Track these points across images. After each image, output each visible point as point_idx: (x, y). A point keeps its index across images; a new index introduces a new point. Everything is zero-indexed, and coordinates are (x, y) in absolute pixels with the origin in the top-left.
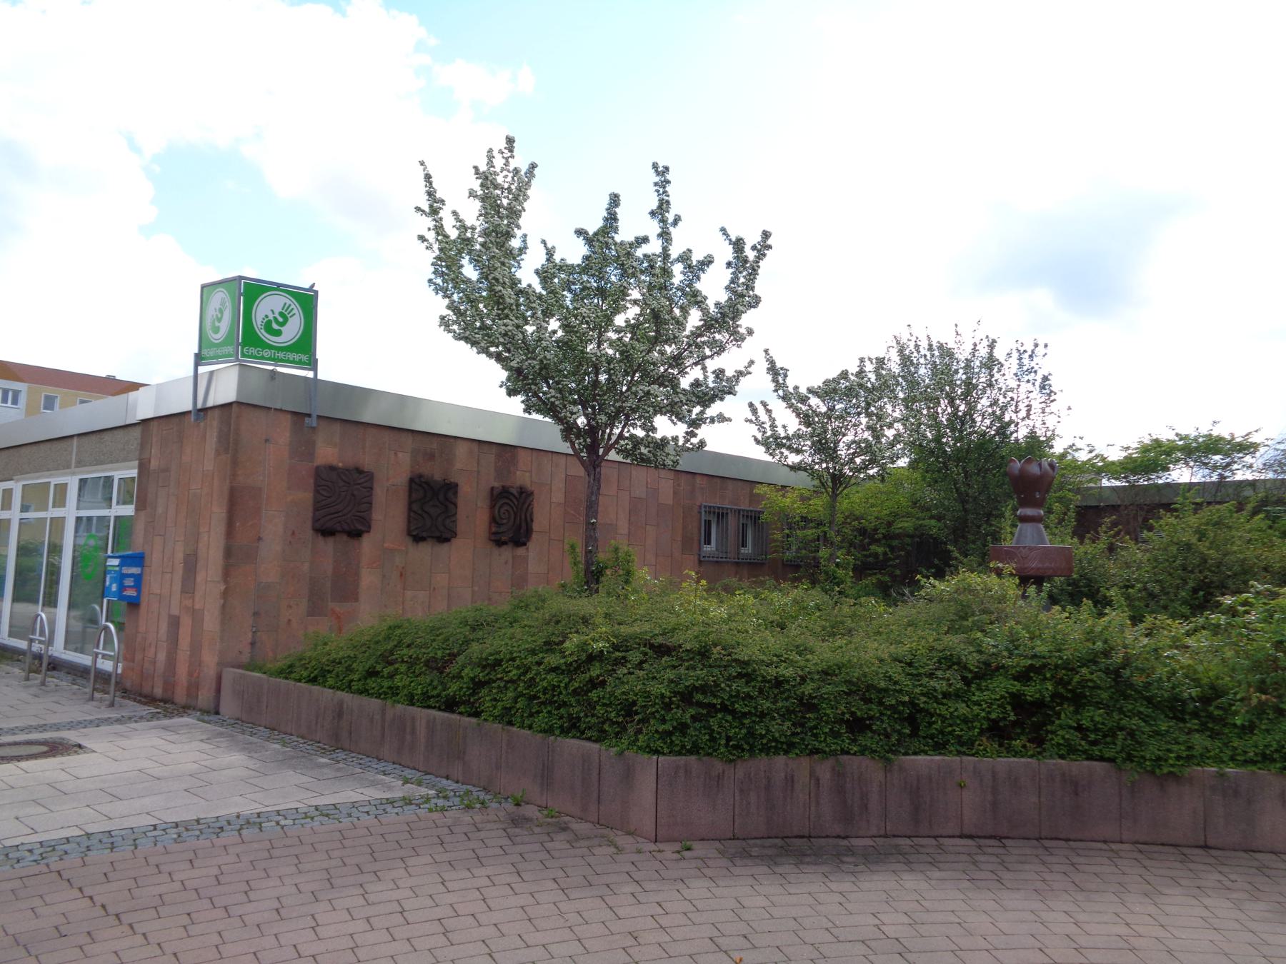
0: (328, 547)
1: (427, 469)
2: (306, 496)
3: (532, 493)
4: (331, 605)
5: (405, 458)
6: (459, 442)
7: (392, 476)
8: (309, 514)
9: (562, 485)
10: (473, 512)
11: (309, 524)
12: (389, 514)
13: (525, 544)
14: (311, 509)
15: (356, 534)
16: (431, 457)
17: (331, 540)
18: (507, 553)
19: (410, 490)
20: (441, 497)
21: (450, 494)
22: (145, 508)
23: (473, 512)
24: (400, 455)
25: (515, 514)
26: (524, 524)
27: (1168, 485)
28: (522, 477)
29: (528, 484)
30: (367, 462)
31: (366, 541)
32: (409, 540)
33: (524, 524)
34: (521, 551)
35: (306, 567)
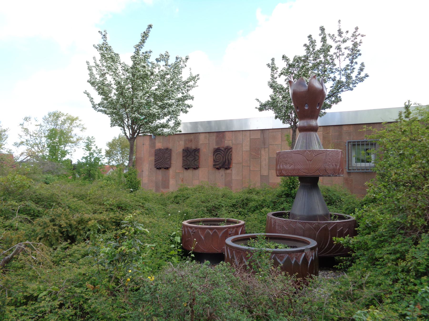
0: (160, 172)
1: (189, 146)
2: (153, 158)
3: (231, 148)
4: (161, 189)
5: (182, 143)
6: (201, 134)
7: (178, 148)
8: (154, 163)
9: (248, 144)
10: (207, 158)
11: (153, 166)
12: (177, 161)
13: (229, 168)
14: (154, 161)
15: (167, 168)
16: (191, 141)
17: (161, 170)
18: (222, 171)
19: (183, 153)
20: (193, 154)
21: (196, 153)
22: (332, 258)
23: (207, 158)
24: (180, 142)
25: (223, 158)
26: (227, 161)
27: (65, 160)
28: (227, 143)
29: (231, 145)
30: (170, 146)
31: (171, 171)
32: (185, 170)
33: (227, 161)
34: (228, 171)
35: (154, 178)
